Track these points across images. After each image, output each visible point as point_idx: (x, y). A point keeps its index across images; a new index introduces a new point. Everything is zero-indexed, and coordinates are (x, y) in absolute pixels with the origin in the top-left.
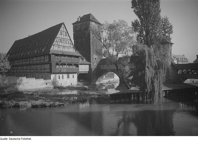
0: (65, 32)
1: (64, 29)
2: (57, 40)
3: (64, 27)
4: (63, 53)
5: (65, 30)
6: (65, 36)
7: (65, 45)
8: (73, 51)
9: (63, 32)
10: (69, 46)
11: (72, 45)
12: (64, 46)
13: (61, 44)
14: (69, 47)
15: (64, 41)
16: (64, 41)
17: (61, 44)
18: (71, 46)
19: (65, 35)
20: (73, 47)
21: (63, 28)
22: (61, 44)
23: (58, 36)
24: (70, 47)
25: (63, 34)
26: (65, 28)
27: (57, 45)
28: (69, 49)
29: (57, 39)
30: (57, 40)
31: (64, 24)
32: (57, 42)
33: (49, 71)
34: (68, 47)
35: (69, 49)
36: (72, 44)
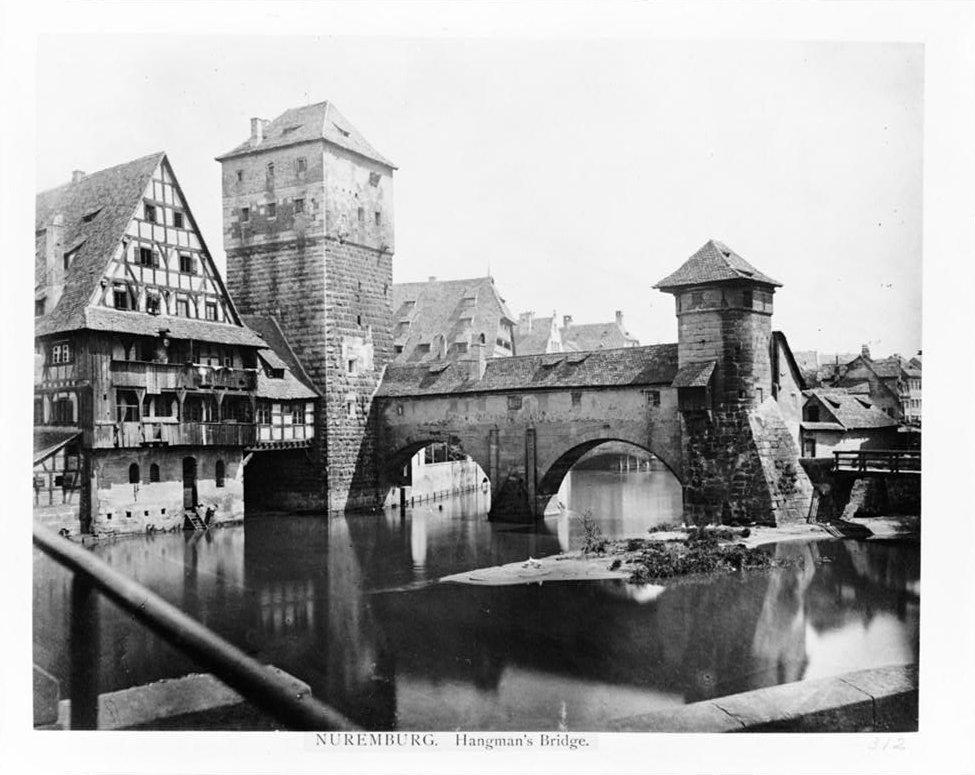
1: (168, 188)
3: (167, 179)
5: (171, 198)
6: (172, 233)
11: (215, 283)
20: (220, 293)
21: (158, 186)
23: (132, 229)
25: (160, 219)
26: (175, 185)
31: (166, 163)
34: (189, 294)
36: (212, 274)
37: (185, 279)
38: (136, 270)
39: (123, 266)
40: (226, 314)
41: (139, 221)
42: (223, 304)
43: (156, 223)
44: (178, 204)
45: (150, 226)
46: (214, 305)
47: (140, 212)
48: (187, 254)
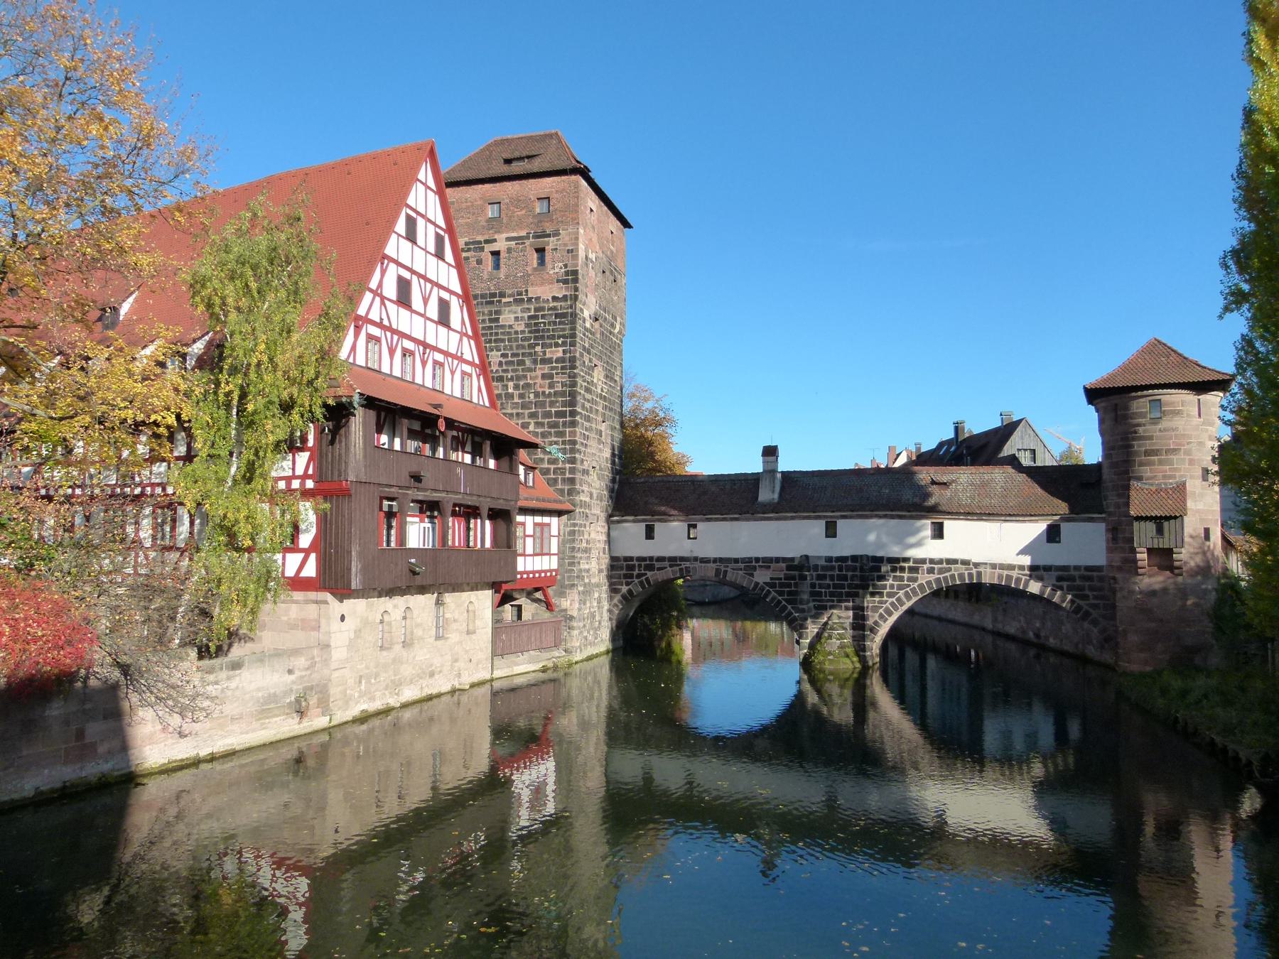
0: (434, 224)
2: (380, 285)
4: (437, 406)
6: (433, 260)
7: (431, 340)
8: (475, 400)
9: (421, 222)
10: (453, 351)
11: (472, 342)
12: (425, 345)
13: (402, 319)
14: (454, 357)
15: (426, 301)
16: (426, 301)
17: (404, 328)
18: (468, 356)
19: (432, 248)
20: (477, 361)
21: (421, 187)
22: (402, 319)
23: (390, 250)
24: (462, 360)
25: (420, 241)
27: (379, 325)
28: (453, 373)
29: (383, 272)
30: (380, 285)
32: (383, 303)
33: (310, 570)
34: (446, 354)
35: (453, 373)
36: (470, 333)
37: (442, 330)
38: (392, 308)
39: (378, 299)
40: (480, 390)
41: (399, 235)
42: (478, 376)
43: (416, 244)
44: (441, 222)
45: (409, 244)
46: (470, 375)
47: (401, 226)
48: (445, 295)
